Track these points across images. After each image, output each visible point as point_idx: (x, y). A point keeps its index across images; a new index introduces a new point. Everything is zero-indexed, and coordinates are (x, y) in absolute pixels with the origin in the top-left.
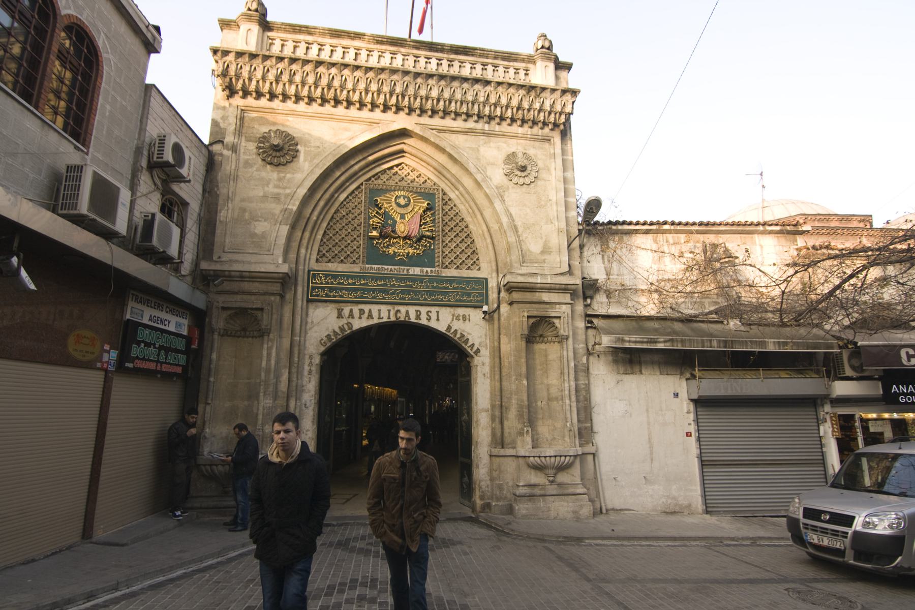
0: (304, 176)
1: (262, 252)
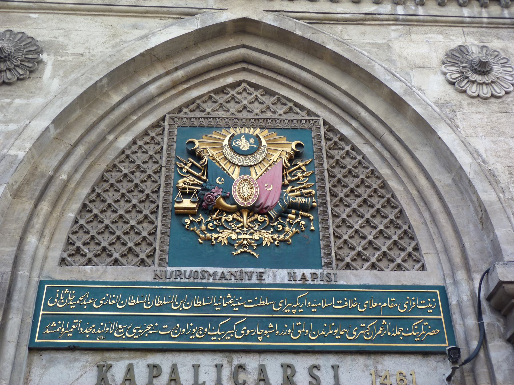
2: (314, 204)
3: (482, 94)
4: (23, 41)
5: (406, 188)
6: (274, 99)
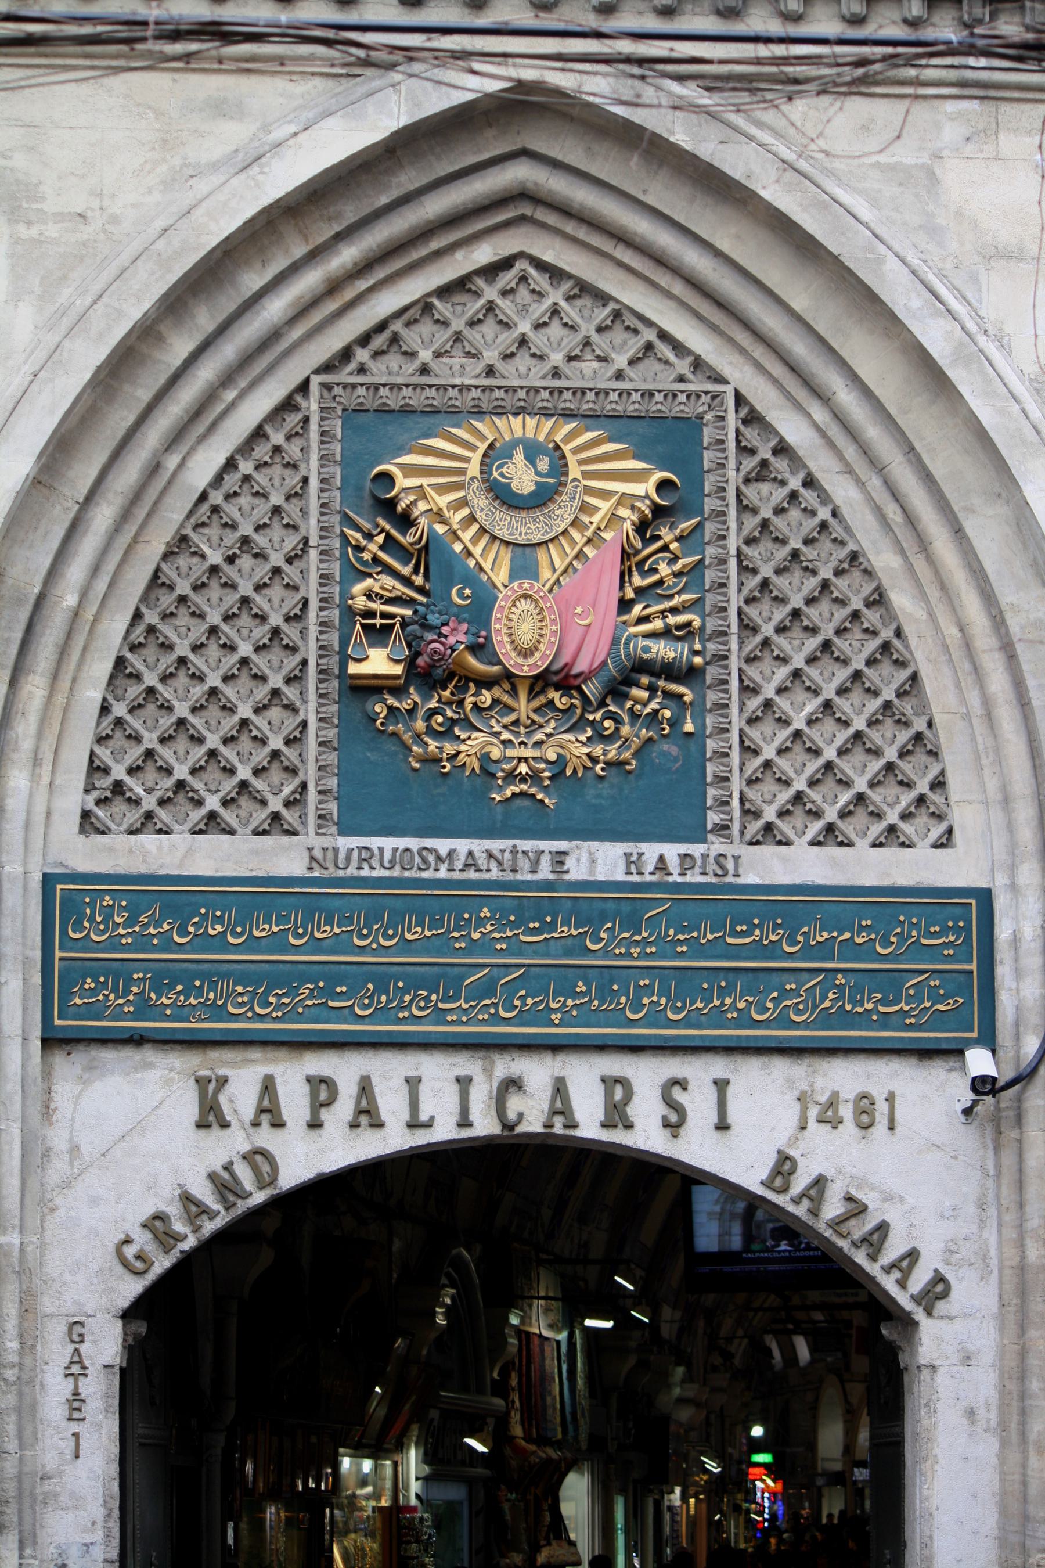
2: (698, 660)
5: (931, 615)
6: (602, 314)
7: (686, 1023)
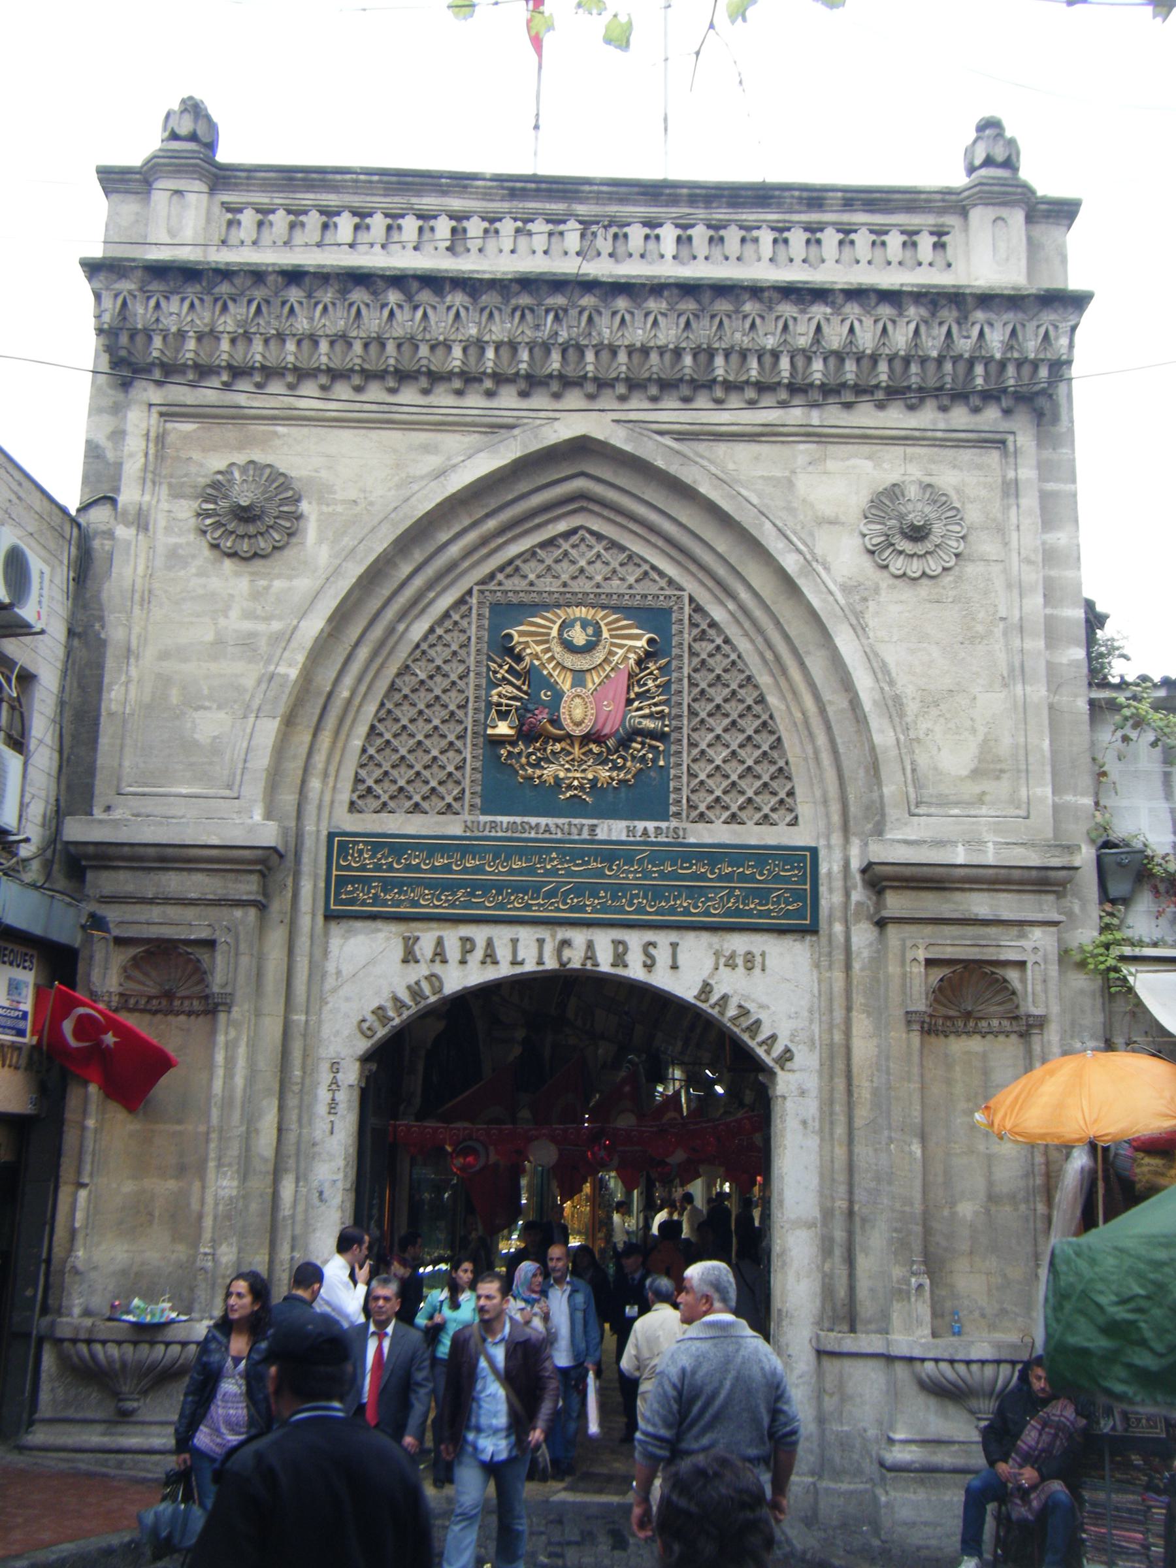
0: (320, 582)
1: (211, 792)
3: (909, 573)
4: (274, 481)
5: (788, 707)
6: (622, 557)
7: (656, 913)
